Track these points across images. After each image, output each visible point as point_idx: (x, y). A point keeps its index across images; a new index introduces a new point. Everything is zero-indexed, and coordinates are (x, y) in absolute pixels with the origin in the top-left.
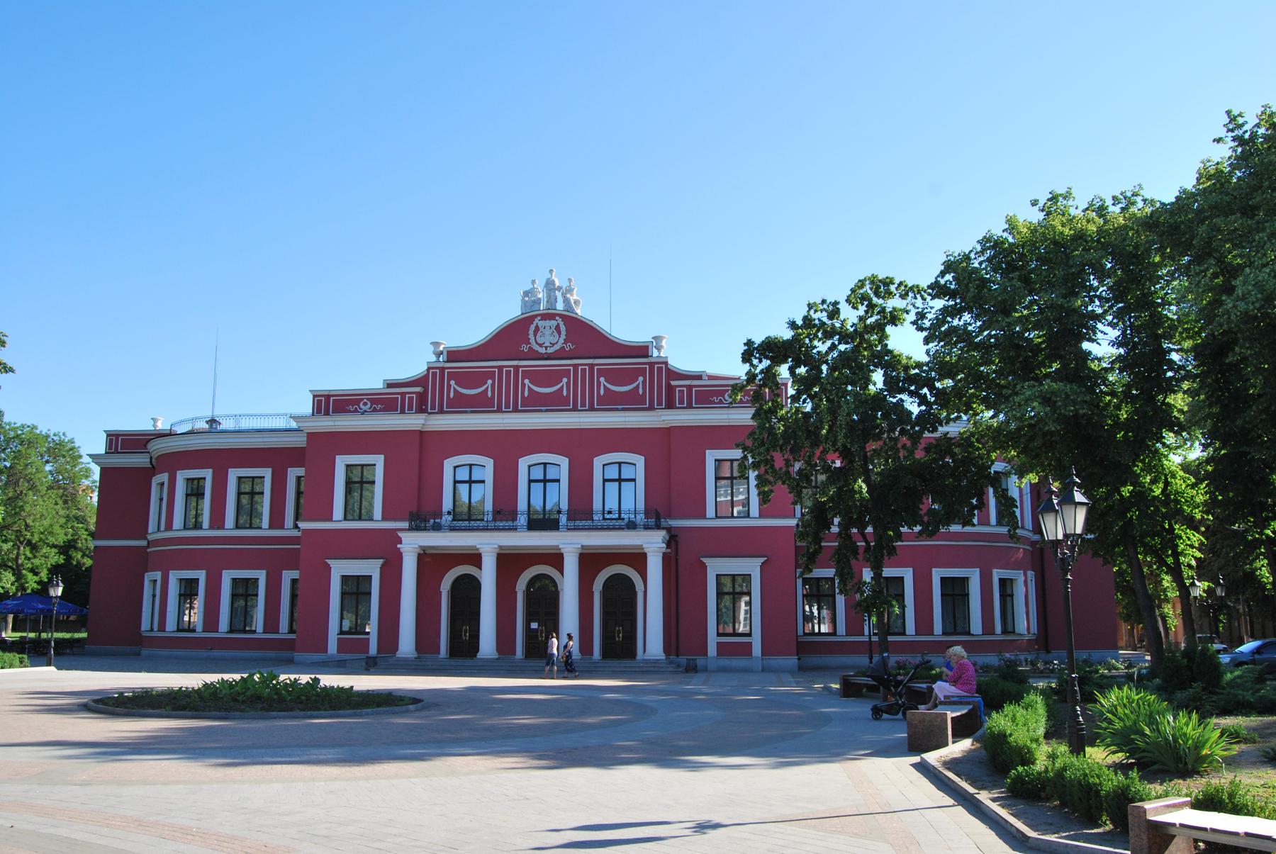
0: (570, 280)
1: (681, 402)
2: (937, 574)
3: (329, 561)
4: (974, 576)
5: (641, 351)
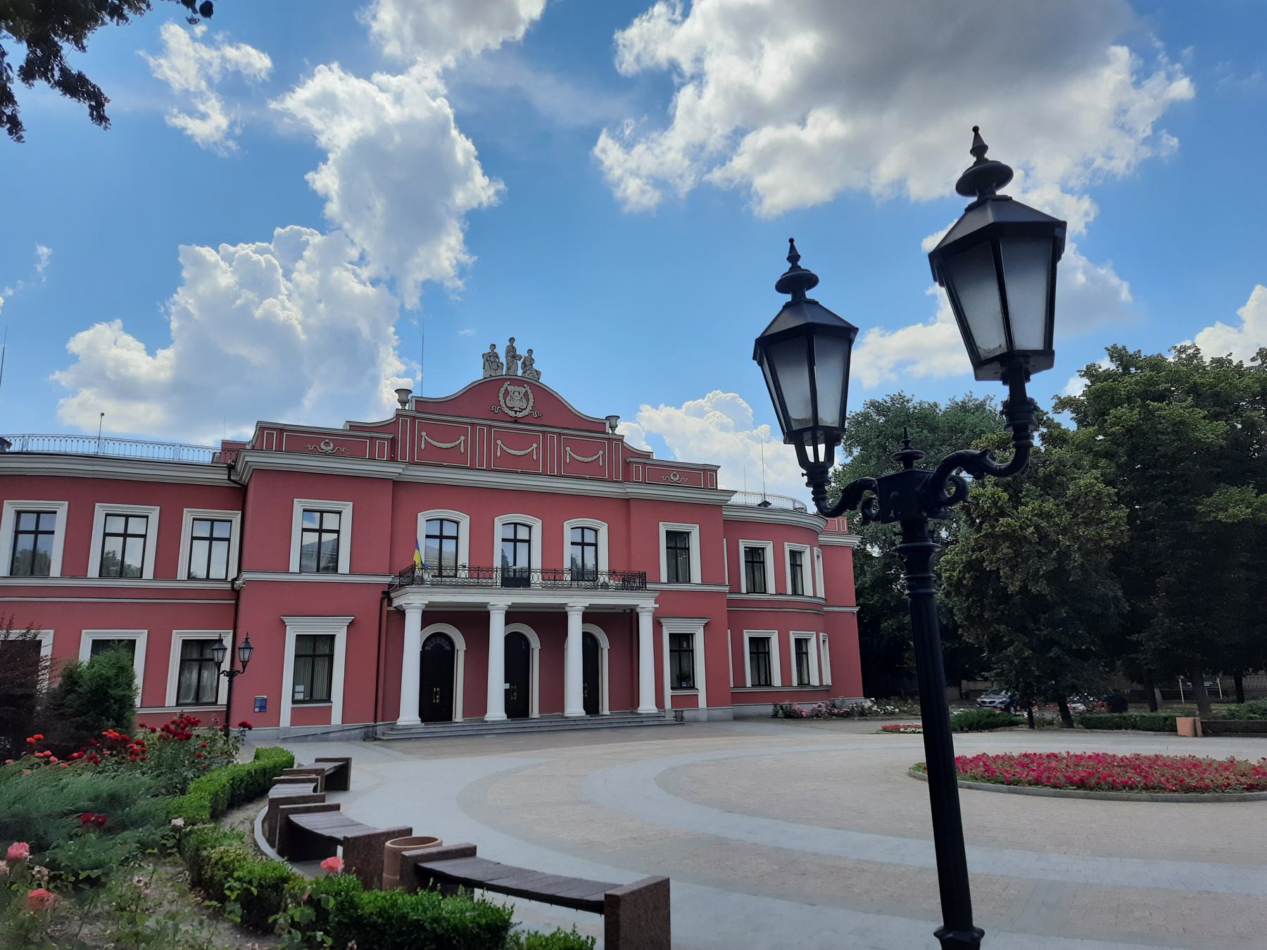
0: (530, 351)
3: (285, 619)
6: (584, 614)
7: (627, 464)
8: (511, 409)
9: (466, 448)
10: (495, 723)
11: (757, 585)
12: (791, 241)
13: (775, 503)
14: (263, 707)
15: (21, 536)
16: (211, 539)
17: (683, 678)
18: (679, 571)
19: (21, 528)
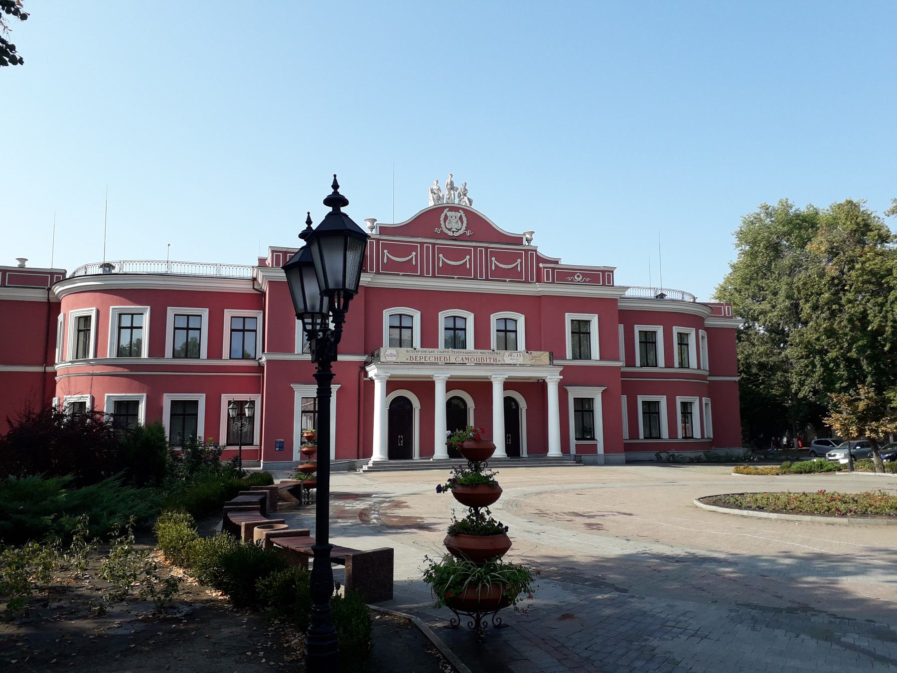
1: (548, 278)
2: (679, 400)
4: (663, 400)
5: (518, 240)
6: (505, 383)
7: (538, 269)
8: (450, 230)
9: (417, 261)
10: (439, 461)
11: (649, 359)
12: (335, 176)
13: (669, 296)
14: (281, 448)
15: (122, 330)
16: (244, 331)
17: (585, 431)
18: (581, 351)
19: (122, 325)
